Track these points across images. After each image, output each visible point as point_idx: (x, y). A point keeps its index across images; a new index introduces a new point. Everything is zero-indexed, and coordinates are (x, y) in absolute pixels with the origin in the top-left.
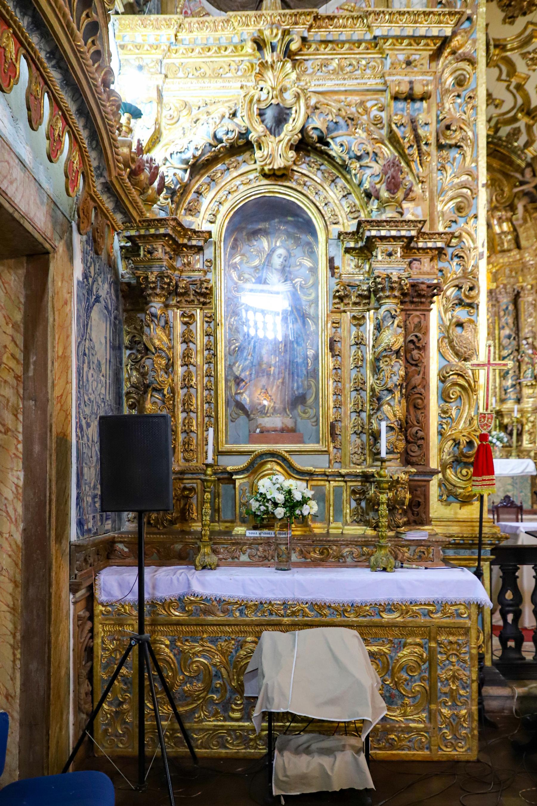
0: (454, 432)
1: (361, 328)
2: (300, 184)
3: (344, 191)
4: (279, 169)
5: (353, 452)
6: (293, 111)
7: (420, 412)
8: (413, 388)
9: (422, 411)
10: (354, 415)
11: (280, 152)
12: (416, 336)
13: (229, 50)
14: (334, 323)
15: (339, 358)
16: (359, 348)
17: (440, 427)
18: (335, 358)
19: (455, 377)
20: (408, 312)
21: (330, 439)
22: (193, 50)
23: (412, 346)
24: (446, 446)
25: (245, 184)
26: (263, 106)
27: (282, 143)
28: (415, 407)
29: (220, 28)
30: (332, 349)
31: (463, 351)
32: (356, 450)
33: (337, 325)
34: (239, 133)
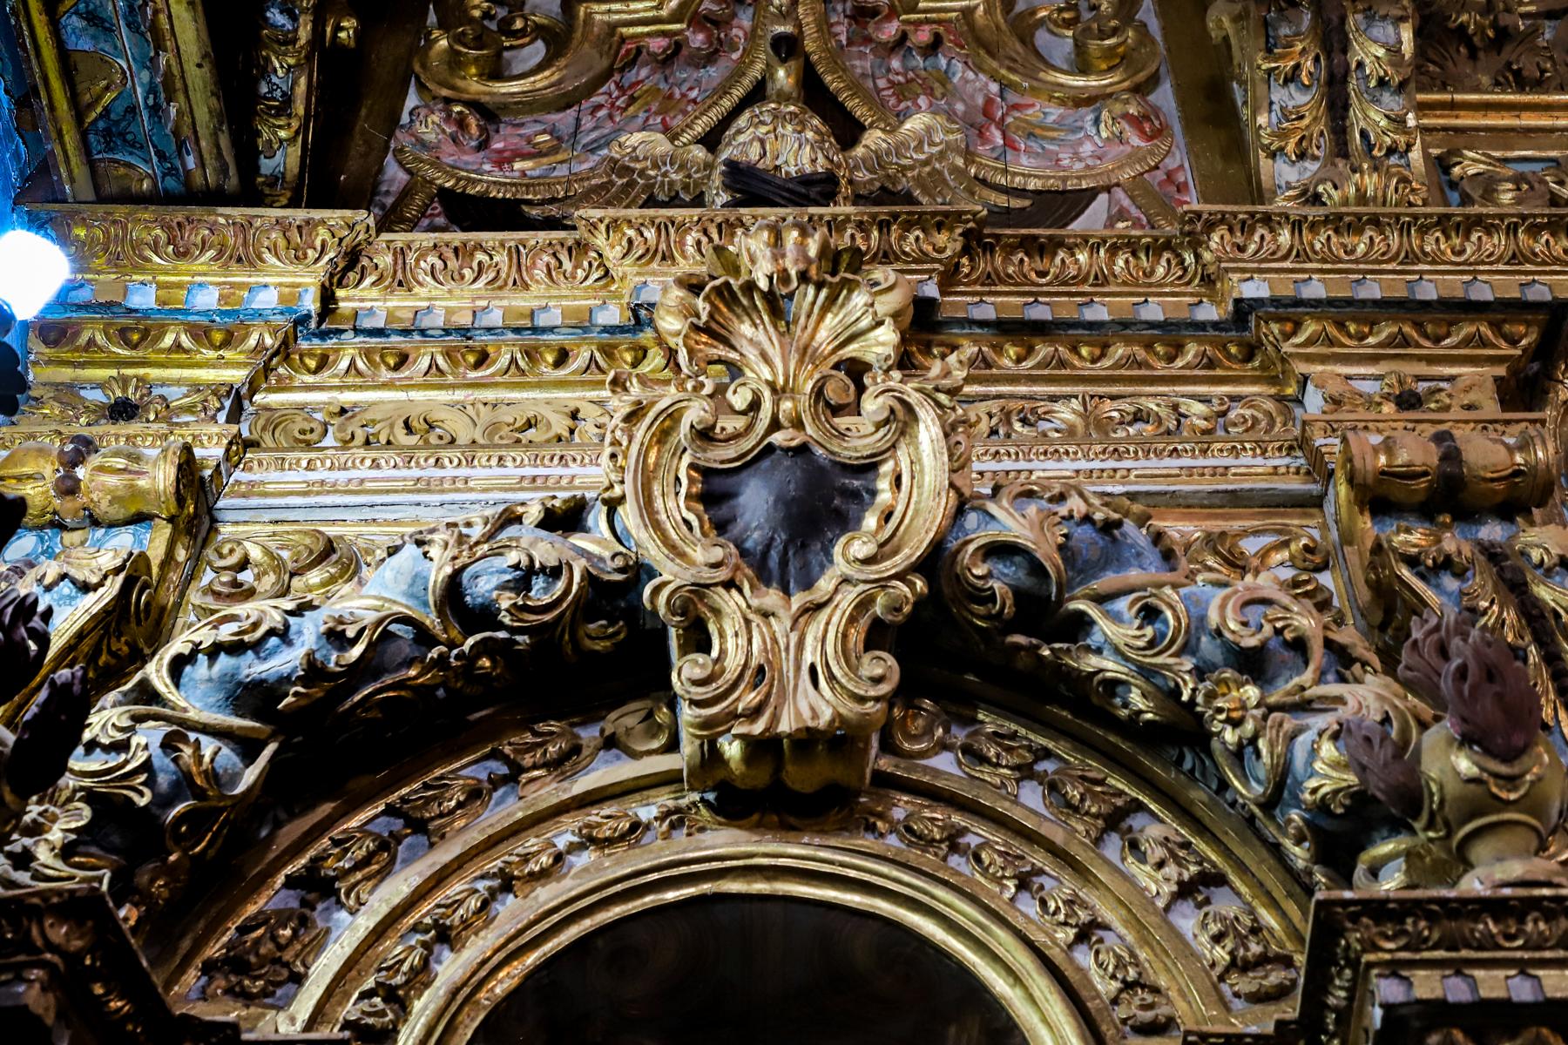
2: (928, 843)
3: (1179, 862)
4: (807, 740)
6: (884, 485)
11: (809, 657)
13: (579, 360)
22: (403, 360)
25: (609, 842)
26: (719, 455)
27: (823, 616)
29: (540, 273)
34: (588, 576)
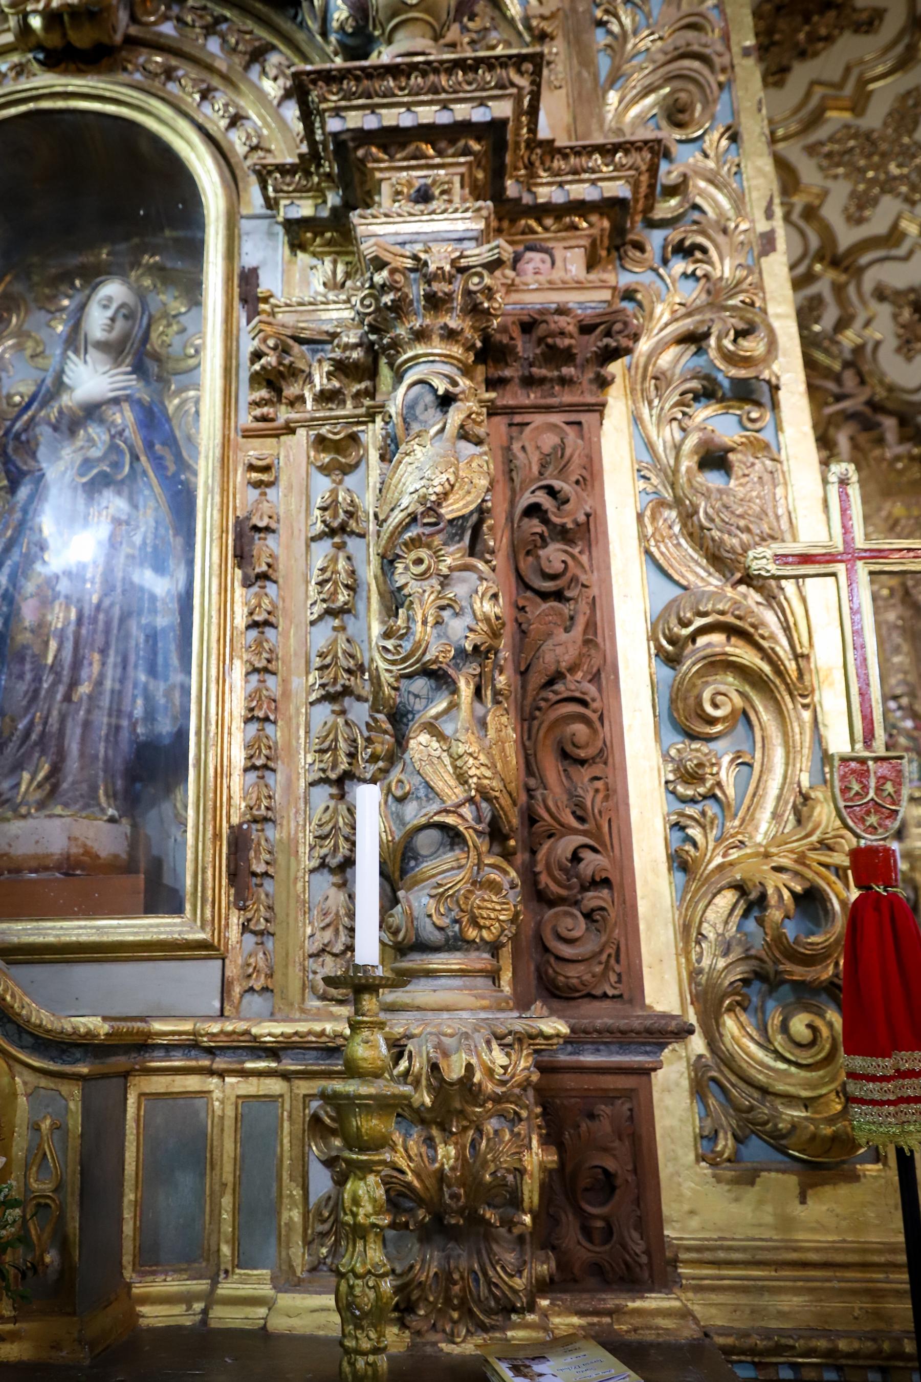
0: (734, 854)
1: (350, 481)
5: (315, 947)
7: (586, 773)
8: (551, 682)
9: (596, 770)
10: (322, 796)
12: (551, 491)
14: (252, 468)
15: (271, 588)
16: (341, 547)
17: (678, 835)
18: (255, 589)
19: (717, 638)
20: (518, 419)
21: (226, 895)
23: (535, 526)
24: (710, 915)
28: (565, 755)
30: (242, 556)
31: (735, 541)
32: (328, 935)
33: (264, 477)
